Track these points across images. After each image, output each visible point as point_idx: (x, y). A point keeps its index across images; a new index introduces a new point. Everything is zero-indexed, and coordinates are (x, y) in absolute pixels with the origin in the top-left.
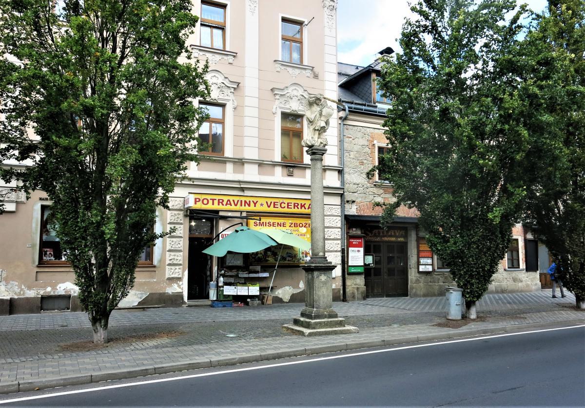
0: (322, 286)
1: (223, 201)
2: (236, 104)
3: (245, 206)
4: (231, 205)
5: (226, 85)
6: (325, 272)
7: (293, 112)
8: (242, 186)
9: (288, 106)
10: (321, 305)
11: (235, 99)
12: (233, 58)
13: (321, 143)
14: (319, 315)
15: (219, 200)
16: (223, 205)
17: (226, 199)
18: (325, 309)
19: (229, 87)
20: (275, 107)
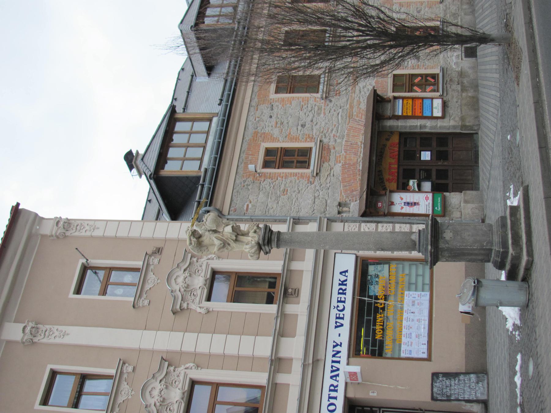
5: (164, 377)
9: (199, 292)
11: (185, 365)
12: (127, 365)
13: (255, 232)
19: (167, 372)
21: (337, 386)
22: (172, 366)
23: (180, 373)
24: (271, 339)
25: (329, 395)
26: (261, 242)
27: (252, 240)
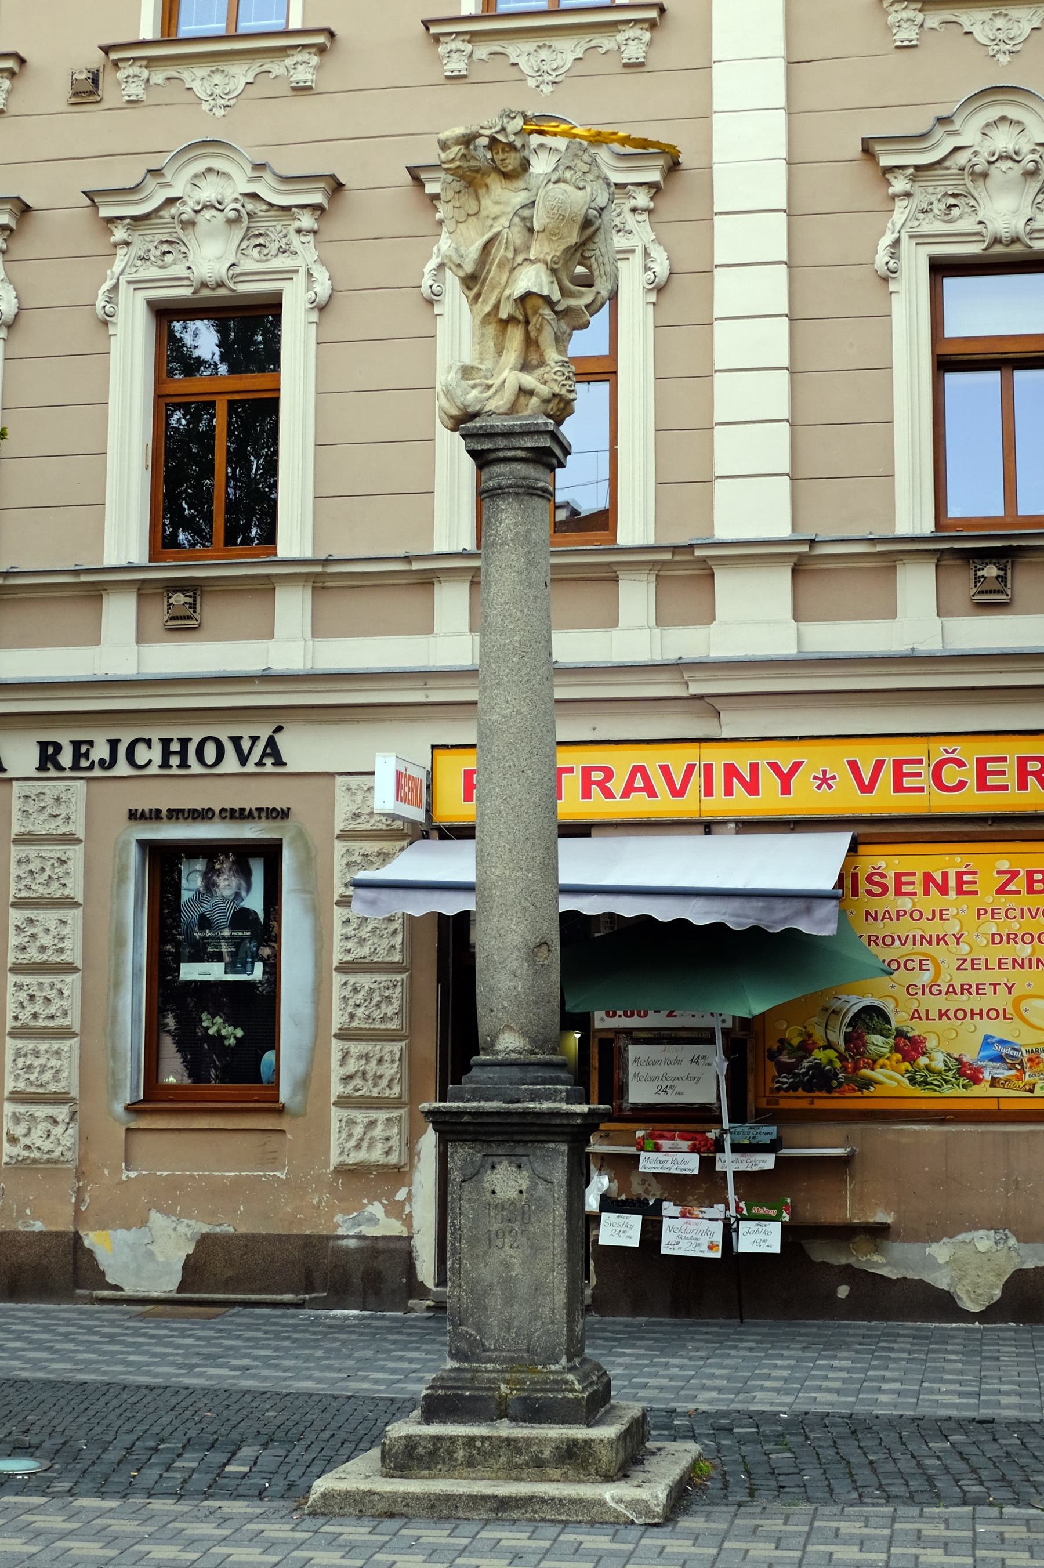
0: (501, 1233)
1: (609, 774)
2: (661, 267)
3: (729, 791)
4: (652, 794)
6: (520, 1150)
7: (998, 249)
8: (695, 689)
10: (489, 1343)
11: (658, 240)
12: (647, 36)
14: (462, 1397)
15: (586, 771)
16: (608, 794)
17: (621, 761)
18: (512, 1363)
20: (888, 239)
22: (652, 199)
24: (784, 531)
26: (477, 423)
27: (489, 387)
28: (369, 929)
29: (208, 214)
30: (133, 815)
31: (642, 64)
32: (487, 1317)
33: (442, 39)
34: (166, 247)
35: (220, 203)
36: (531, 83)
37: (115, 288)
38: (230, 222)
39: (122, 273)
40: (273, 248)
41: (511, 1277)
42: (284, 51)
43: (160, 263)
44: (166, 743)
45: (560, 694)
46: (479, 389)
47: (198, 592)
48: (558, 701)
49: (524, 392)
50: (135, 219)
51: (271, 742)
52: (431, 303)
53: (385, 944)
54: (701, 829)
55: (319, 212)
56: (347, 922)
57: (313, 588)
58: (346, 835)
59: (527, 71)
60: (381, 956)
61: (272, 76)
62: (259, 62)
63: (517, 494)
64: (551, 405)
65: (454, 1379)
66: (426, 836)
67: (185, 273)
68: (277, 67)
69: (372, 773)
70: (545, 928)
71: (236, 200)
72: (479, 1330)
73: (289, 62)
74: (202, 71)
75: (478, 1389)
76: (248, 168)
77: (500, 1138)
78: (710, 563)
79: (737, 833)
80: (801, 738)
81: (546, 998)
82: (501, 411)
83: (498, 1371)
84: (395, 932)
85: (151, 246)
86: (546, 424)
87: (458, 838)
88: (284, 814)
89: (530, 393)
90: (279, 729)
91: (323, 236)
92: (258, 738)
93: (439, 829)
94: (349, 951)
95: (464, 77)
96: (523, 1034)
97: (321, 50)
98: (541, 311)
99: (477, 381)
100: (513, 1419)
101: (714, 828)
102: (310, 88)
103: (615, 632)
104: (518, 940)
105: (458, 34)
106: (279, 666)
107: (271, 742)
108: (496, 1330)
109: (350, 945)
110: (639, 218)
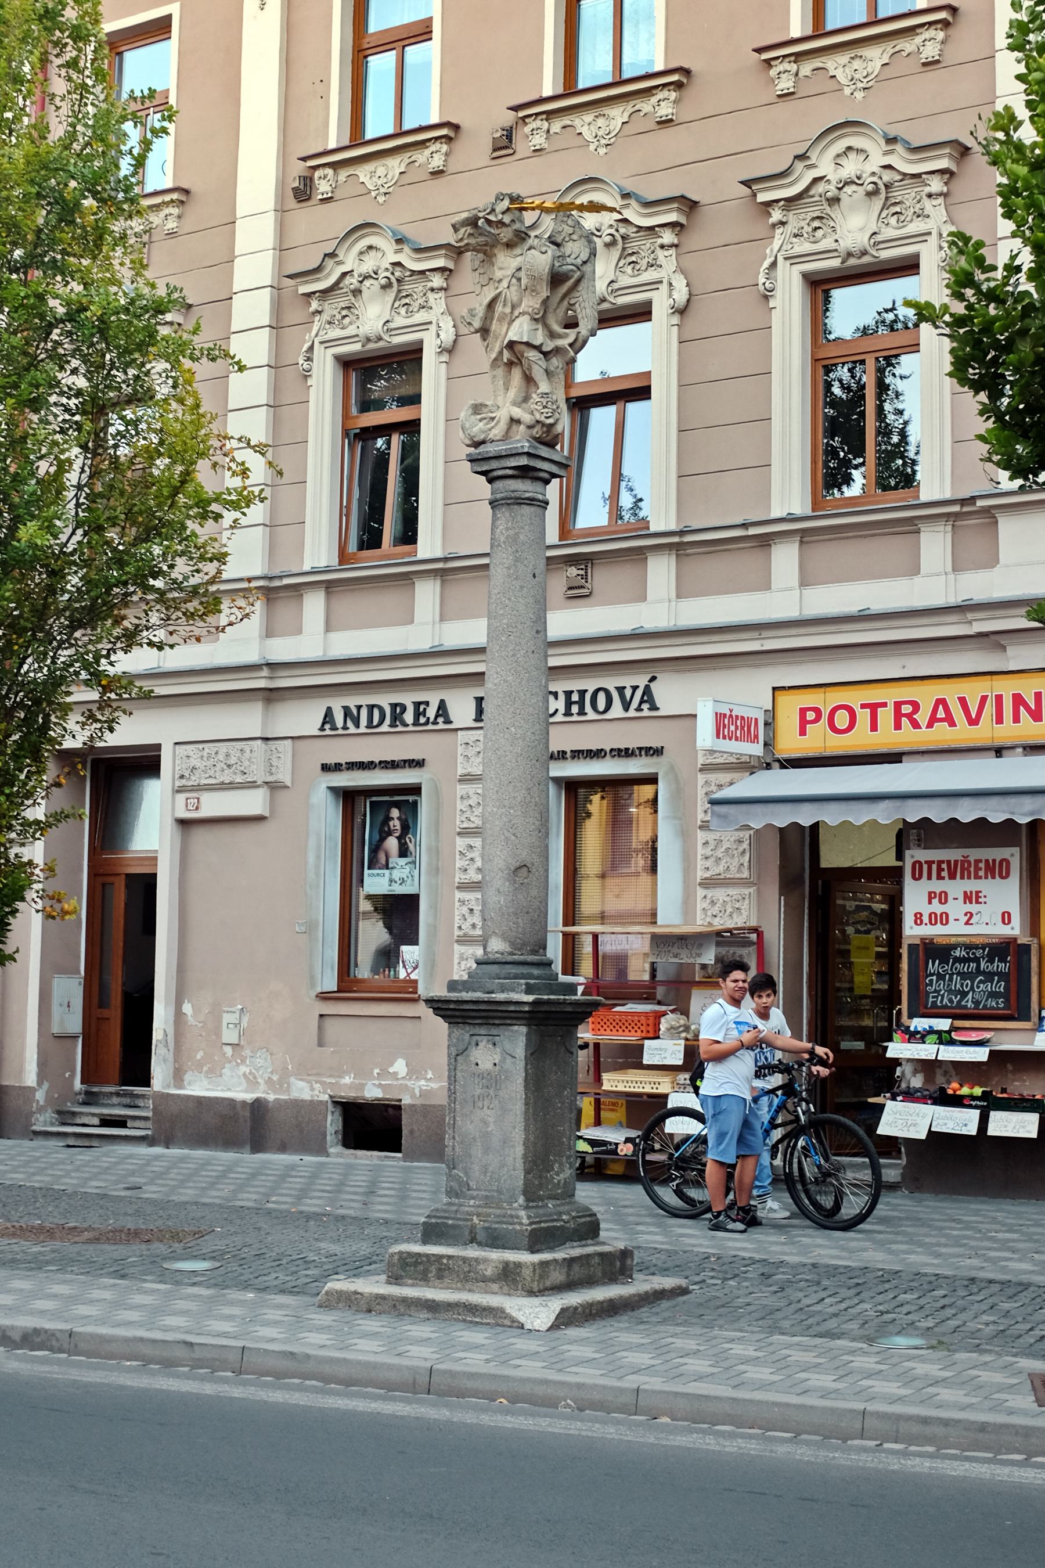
1: (916, 706)
3: (1016, 719)
4: (952, 724)
6: (494, 1031)
12: (941, 35)
14: (446, 1225)
15: (898, 705)
16: (916, 725)
17: (926, 695)
21: (916, 725)
22: (946, 184)
23: (928, 216)
25: (884, 705)
28: (723, 850)
29: (849, 189)
30: (326, 768)
31: (938, 62)
32: (472, 1163)
33: (773, 63)
34: (816, 224)
35: (598, 231)
36: (847, 91)
37: (774, 265)
38: (869, 194)
39: (779, 251)
40: (644, 263)
41: (487, 1132)
42: (912, 30)
43: (812, 239)
44: (568, 694)
45: (552, 662)
46: (485, 421)
47: (590, 565)
48: (551, 668)
49: (514, 421)
50: (788, 200)
51: (647, 691)
52: (766, 298)
53: (735, 862)
54: (994, 753)
55: (678, 228)
56: (706, 843)
57: (677, 555)
58: (705, 769)
59: (843, 80)
60: (733, 874)
61: (417, 164)
62: (632, 103)
63: (508, 504)
64: (535, 430)
65: (445, 1211)
66: (768, 766)
67: (834, 246)
68: (645, 105)
69: (695, 716)
70: (525, 853)
71: (611, 226)
72: (466, 1174)
73: (654, 100)
74: (588, 117)
75: (460, 1219)
76: (882, 142)
77: (480, 1021)
78: (993, 512)
79: (1026, 755)
80: (790, 688)
81: (525, 910)
82: (498, 438)
83: (479, 1206)
84: (744, 852)
85: (803, 224)
86: (522, 447)
87: (793, 767)
88: (658, 752)
89: (518, 422)
90: (653, 679)
91: (683, 249)
92: (638, 687)
93: (778, 761)
94: (707, 869)
95: (793, 93)
96: (504, 938)
97: (945, 24)
98: (525, 355)
99: (483, 416)
100: (480, 1244)
101: (1004, 752)
102: (671, 120)
103: (917, 579)
104: (501, 864)
105: (784, 56)
106: (650, 625)
107: (647, 691)
108: (477, 1173)
109: (708, 864)
110: (935, 202)
